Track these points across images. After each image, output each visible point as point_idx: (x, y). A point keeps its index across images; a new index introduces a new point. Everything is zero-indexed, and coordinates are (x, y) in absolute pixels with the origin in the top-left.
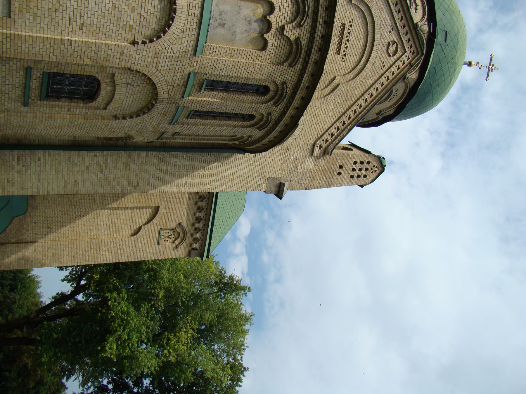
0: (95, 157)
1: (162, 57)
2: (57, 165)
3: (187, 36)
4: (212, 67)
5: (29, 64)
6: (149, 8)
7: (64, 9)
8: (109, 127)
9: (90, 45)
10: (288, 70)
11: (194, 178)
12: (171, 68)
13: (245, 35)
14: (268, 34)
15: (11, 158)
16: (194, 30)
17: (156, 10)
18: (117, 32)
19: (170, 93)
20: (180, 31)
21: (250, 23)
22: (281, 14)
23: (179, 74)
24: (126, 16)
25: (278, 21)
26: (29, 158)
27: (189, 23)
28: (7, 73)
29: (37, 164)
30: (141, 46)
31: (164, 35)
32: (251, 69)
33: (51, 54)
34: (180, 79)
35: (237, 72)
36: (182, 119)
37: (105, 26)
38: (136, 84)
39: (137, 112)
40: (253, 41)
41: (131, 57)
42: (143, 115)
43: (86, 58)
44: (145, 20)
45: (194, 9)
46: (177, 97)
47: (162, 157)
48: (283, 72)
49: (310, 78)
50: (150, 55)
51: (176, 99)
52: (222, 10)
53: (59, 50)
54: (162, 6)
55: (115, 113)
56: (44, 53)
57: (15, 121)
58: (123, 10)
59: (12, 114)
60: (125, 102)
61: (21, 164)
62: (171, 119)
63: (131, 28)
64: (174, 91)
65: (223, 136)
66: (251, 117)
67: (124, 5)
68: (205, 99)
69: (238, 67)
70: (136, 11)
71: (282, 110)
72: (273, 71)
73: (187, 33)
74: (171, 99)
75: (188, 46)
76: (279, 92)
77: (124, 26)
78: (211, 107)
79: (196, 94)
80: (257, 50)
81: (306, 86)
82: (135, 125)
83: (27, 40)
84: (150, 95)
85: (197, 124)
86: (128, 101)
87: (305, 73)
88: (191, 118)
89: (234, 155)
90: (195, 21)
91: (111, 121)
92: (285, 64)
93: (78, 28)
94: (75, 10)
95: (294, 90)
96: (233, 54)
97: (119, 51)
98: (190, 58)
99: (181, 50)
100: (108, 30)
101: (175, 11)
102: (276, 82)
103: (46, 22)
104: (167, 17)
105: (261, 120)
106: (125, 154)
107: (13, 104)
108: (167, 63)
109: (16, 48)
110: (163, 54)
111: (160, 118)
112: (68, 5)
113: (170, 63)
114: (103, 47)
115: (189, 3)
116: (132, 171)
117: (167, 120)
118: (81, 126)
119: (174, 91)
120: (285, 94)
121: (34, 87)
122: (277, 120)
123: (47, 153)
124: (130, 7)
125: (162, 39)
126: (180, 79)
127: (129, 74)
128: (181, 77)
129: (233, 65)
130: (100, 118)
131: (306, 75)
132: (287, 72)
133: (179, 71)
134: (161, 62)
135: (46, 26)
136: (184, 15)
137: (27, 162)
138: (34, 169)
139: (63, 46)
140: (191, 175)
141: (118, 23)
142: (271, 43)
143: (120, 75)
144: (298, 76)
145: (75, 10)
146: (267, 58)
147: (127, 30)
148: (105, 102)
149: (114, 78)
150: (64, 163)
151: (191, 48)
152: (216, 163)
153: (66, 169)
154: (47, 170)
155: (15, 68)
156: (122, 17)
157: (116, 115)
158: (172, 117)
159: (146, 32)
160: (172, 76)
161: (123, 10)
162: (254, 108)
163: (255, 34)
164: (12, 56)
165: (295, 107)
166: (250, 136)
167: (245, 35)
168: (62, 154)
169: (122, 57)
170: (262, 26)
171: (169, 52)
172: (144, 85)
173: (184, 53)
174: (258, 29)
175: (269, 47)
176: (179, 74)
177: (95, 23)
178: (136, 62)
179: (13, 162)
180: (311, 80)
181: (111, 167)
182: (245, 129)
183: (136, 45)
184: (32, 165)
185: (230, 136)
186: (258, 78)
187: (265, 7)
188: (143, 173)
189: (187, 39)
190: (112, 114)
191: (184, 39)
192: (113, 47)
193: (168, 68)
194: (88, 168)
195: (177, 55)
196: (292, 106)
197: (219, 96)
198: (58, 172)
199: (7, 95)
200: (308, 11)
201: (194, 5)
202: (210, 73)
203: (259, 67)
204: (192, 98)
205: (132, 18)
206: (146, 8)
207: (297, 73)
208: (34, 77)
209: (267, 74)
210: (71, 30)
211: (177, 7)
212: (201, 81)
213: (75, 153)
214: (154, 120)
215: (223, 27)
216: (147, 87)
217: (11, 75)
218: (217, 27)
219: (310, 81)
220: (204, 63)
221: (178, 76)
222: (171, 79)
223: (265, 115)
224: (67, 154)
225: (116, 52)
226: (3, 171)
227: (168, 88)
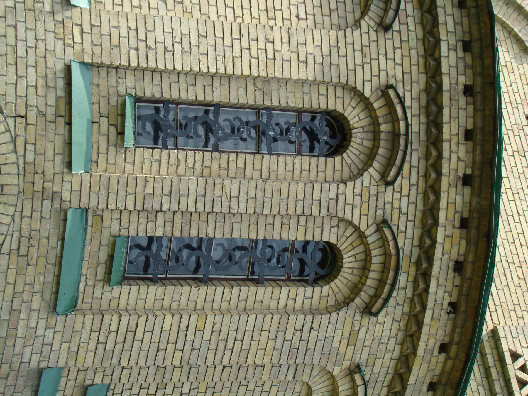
4: (133, 44)
10: (381, 42)
19: (21, 152)
23: (31, 71)
34: (40, 91)
35: (220, 59)
48: (366, 50)
49: (461, 54)
51: (49, 176)
62: (50, 278)
64: (32, 140)
69: (219, 41)
71: (420, 206)
76: (383, 127)
81: (461, 87)
87: (438, 41)
92: (363, 23)
95: (428, 116)
98: (53, 13)
102: (359, 88)
105: (365, 268)
117: (37, 287)
119: (32, 140)
120: (402, 124)
122: (419, 258)
126: (40, 91)
128: (41, 82)
129: (199, 35)
131: (444, 46)
132: (382, 51)
133: (31, 62)
144: (421, 60)
146: (302, 15)
158: (52, 270)
160: (12, 79)
162: (324, 203)
165: (458, 178)
176: (31, 71)
180: (469, 60)
182: (325, 317)
196: (445, 171)
200: (407, 134)
203: (285, 39)
207: (414, 52)
209: (319, 60)
212: (114, 100)
219: (466, 66)
220: (105, 30)
221: (32, 80)
227: (8, 130)
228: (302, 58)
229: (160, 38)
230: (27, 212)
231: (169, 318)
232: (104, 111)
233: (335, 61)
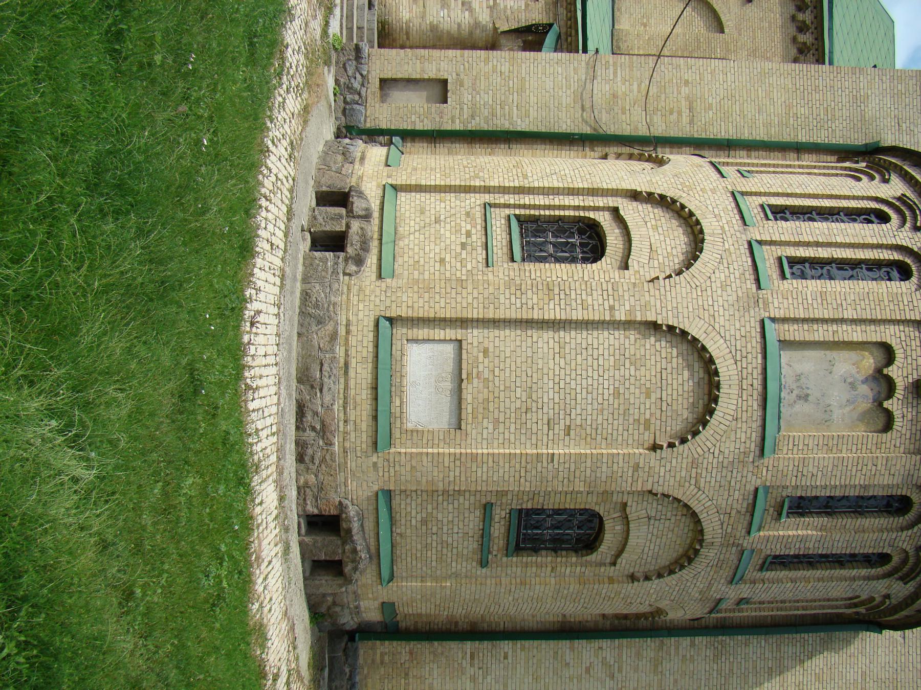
0: (600, 652)
1: (705, 466)
2: (535, 666)
3: (744, 424)
4: (795, 474)
5: (489, 499)
6: (675, 387)
7: (540, 406)
8: (622, 595)
9: (583, 459)
11: (785, 685)
12: (722, 484)
13: (848, 409)
14: (890, 401)
15: (460, 655)
16: (755, 413)
17: (686, 389)
18: (625, 433)
19: (725, 528)
20: (730, 418)
21: (853, 386)
22: (909, 362)
23: (737, 492)
24: (637, 406)
25: (905, 375)
26: (489, 654)
27: (745, 403)
28: (456, 515)
29: (502, 665)
30: (666, 452)
31: (704, 428)
32: (869, 468)
33: (522, 480)
35: (843, 477)
36: (751, 573)
37: (605, 426)
38: (663, 517)
39: (669, 566)
40: (864, 417)
41: (652, 472)
42: (680, 570)
43: (577, 480)
44: (669, 408)
45: (750, 377)
46: (738, 535)
47: (720, 647)
50: (684, 466)
51: (737, 537)
52: (799, 372)
53: (534, 472)
54: (696, 380)
55: (631, 570)
56: (512, 479)
57: (468, 592)
58: (632, 397)
59: (463, 581)
60: (646, 549)
61: (476, 666)
62: (731, 573)
63: (647, 424)
64: (731, 523)
65: (832, 600)
66: (884, 558)
67: (632, 387)
68: (790, 533)
69: (845, 468)
70: (653, 396)
72: (912, 467)
73: (744, 419)
74: (727, 538)
75: (748, 442)
77: (636, 422)
78: (802, 546)
79: (772, 526)
80: (874, 432)
82: (667, 589)
83: (485, 460)
84: (690, 535)
85: (779, 581)
86: (652, 548)
88: (767, 570)
89: (860, 636)
90: (755, 397)
91: (625, 585)
93: (562, 433)
94: (556, 406)
96: (830, 445)
97: (631, 464)
98: (753, 462)
99: (737, 451)
100: (610, 431)
101: (718, 386)
103: (512, 430)
104: (706, 397)
105: (905, 561)
106: (653, 644)
107: (464, 564)
108: (714, 475)
109: (468, 475)
110: (705, 461)
111: (712, 573)
112: (546, 400)
113: (719, 474)
114: (605, 460)
115: (739, 369)
116: (668, 676)
118: (574, 596)
119: (731, 523)
121: (496, 534)
123: (519, 645)
124: (644, 390)
125: (701, 435)
127: (650, 501)
128: (741, 497)
130: (606, 580)
133: (737, 488)
134: (703, 475)
135: (512, 436)
136: (735, 391)
137: (485, 662)
138: (498, 673)
139: (540, 465)
140: (778, 678)
141: (626, 418)
142: (900, 416)
143: (634, 504)
145: (556, 406)
146: (898, 445)
147: (642, 427)
148: (613, 553)
149: (625, 510)
150: (547, 662)
151: (753, 445)
152: (825, 653)
153: (551, 674)
154: (518, 676)
155: (467, 506)
156: (632, 406)
157: (633, 574)
159: (674, 428)
160: (726, 497)
161: (632, 397)
163: (866, 405)
164: (463, 488)
166: (887, 596)
167: (848, 409)
168: (543, 646)
169: (636, 473)
170: (877, 389)
171: (716, 455)
172: (678, 518)
173: (742, 456)
174: (871, 395)
175: (898, 423)
176: (737, 492)
177: (589, 422)
178: (661, 479)
179: (464, 662)
181: (629, 667)
182: (875, 582)
183: (658, 451)
184: (493, 666)
185: (846, 599)
186: (885, 483)
187: (875, 354)
188: (687, 677)
189: (744, 430)
190: (626, 573)
191: (739, 431)
192: (621, 457)
193: (718, 484)
194: (588, 670)
195: (731, 460)
197: (815, 524)
198: (536, 679)
199: (455, 551)
201: (750, 370)
202: (793, 484)
203: (884, 463)
204: (766, 533)
205: (648, 407)
206: (670, 387)
208: (497, 518)
210: (551, 437)
211: (721, 379)
212: (778, 500)
213: (565, 645)
214: (700, 579)
215: (806, 400)
216: (683, 520)
217: (461, 517)
218: (795, 402)
220: (780, 468)
222: (725, 502)
223: (911, 553)
224: (552, 646)
225: (626, 465)
226: (448, 678)
228: (892, 472)
229: (811, 469)
230: (724, 551)
231: (789, 584)
232: (773, 504)
233: (911, 473)
